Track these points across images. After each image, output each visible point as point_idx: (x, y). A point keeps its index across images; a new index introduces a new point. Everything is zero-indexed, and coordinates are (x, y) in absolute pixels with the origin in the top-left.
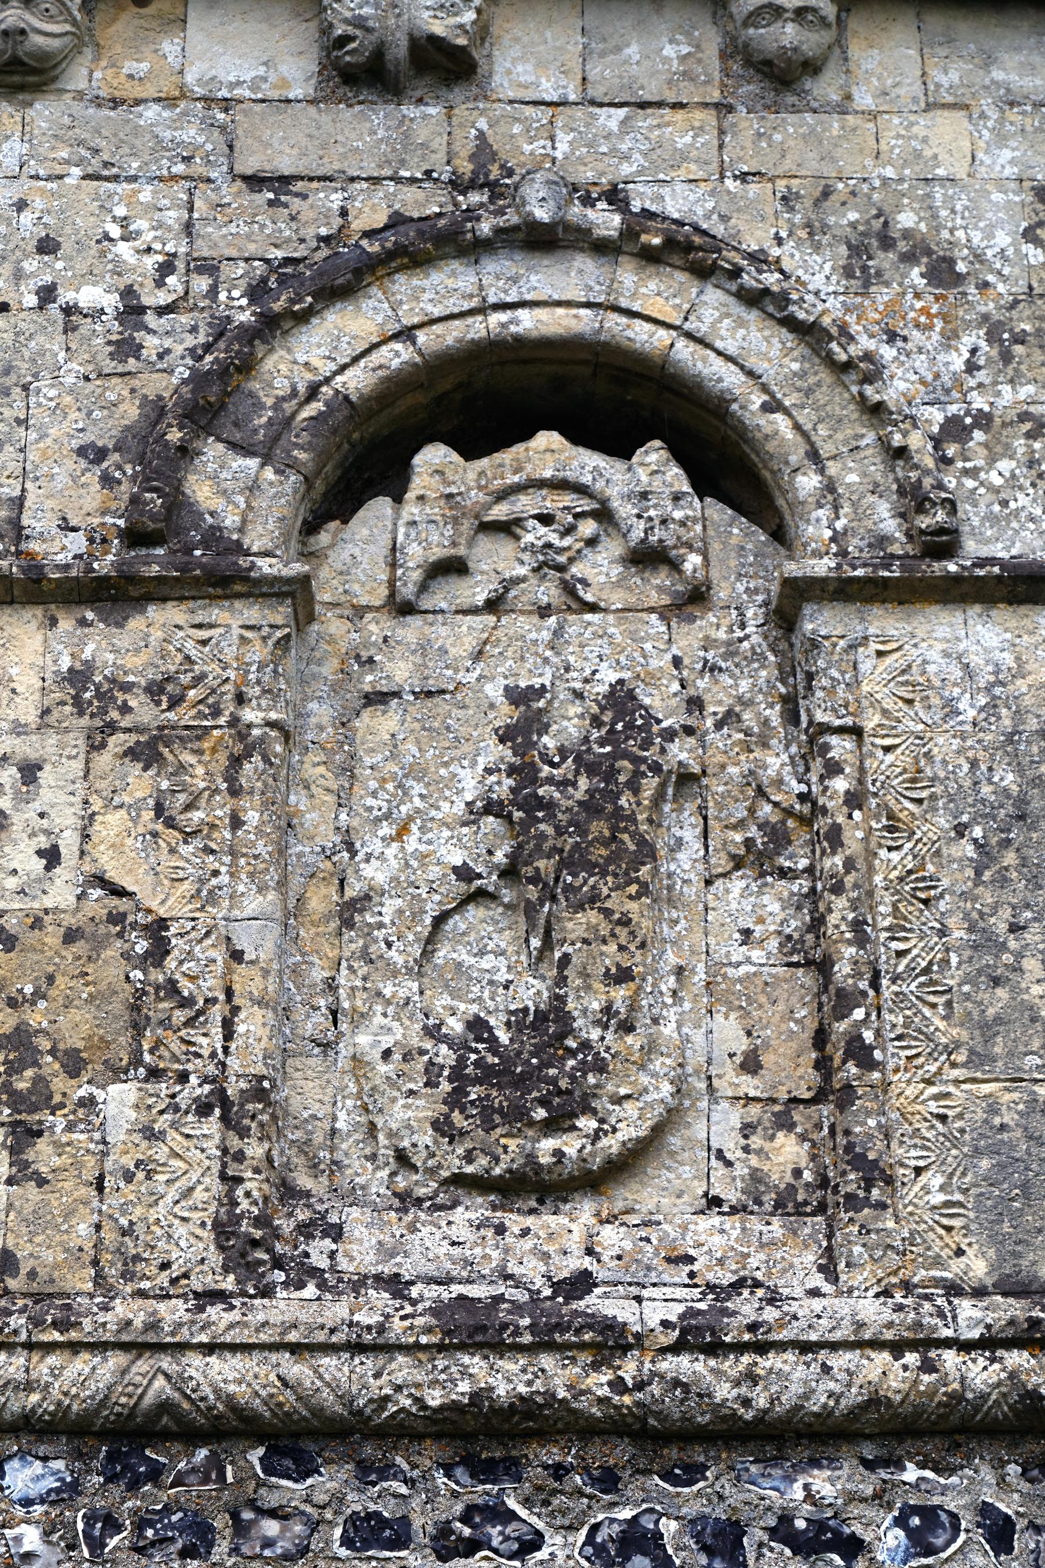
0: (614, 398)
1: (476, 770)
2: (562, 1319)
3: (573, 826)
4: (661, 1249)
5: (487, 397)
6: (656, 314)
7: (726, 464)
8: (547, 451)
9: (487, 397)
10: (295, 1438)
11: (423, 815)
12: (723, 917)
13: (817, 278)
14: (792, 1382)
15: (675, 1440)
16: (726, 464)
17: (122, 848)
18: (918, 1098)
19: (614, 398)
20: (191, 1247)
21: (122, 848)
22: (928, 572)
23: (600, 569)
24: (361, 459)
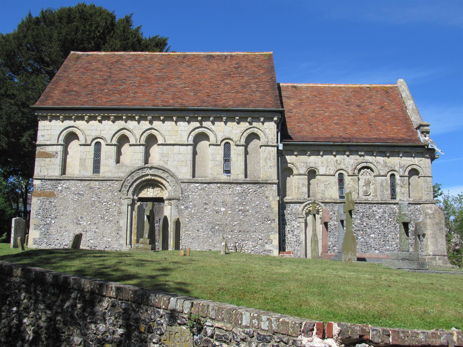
0: (368, 168)
1: (364, 181)
2: (367, 200)
3: (368, 183)
4: (370, 198)
5: (363, 168)
6: (369, 165)
7: (372, 170)
8: (366, 170)
9: (363, 168)
10: (360, 203)
11: (362, 182)
12: (372, 187)
13: (375, 164)
14: (374, 202)
15: (371, 203)
16: (372, 170)
17: (353, 185)
18: (379, 193)
19: (368, 168)
20: (356, 197)
21: (353, 185)
22: (379, 176)
23: (368, 174)
24: (360, 170)
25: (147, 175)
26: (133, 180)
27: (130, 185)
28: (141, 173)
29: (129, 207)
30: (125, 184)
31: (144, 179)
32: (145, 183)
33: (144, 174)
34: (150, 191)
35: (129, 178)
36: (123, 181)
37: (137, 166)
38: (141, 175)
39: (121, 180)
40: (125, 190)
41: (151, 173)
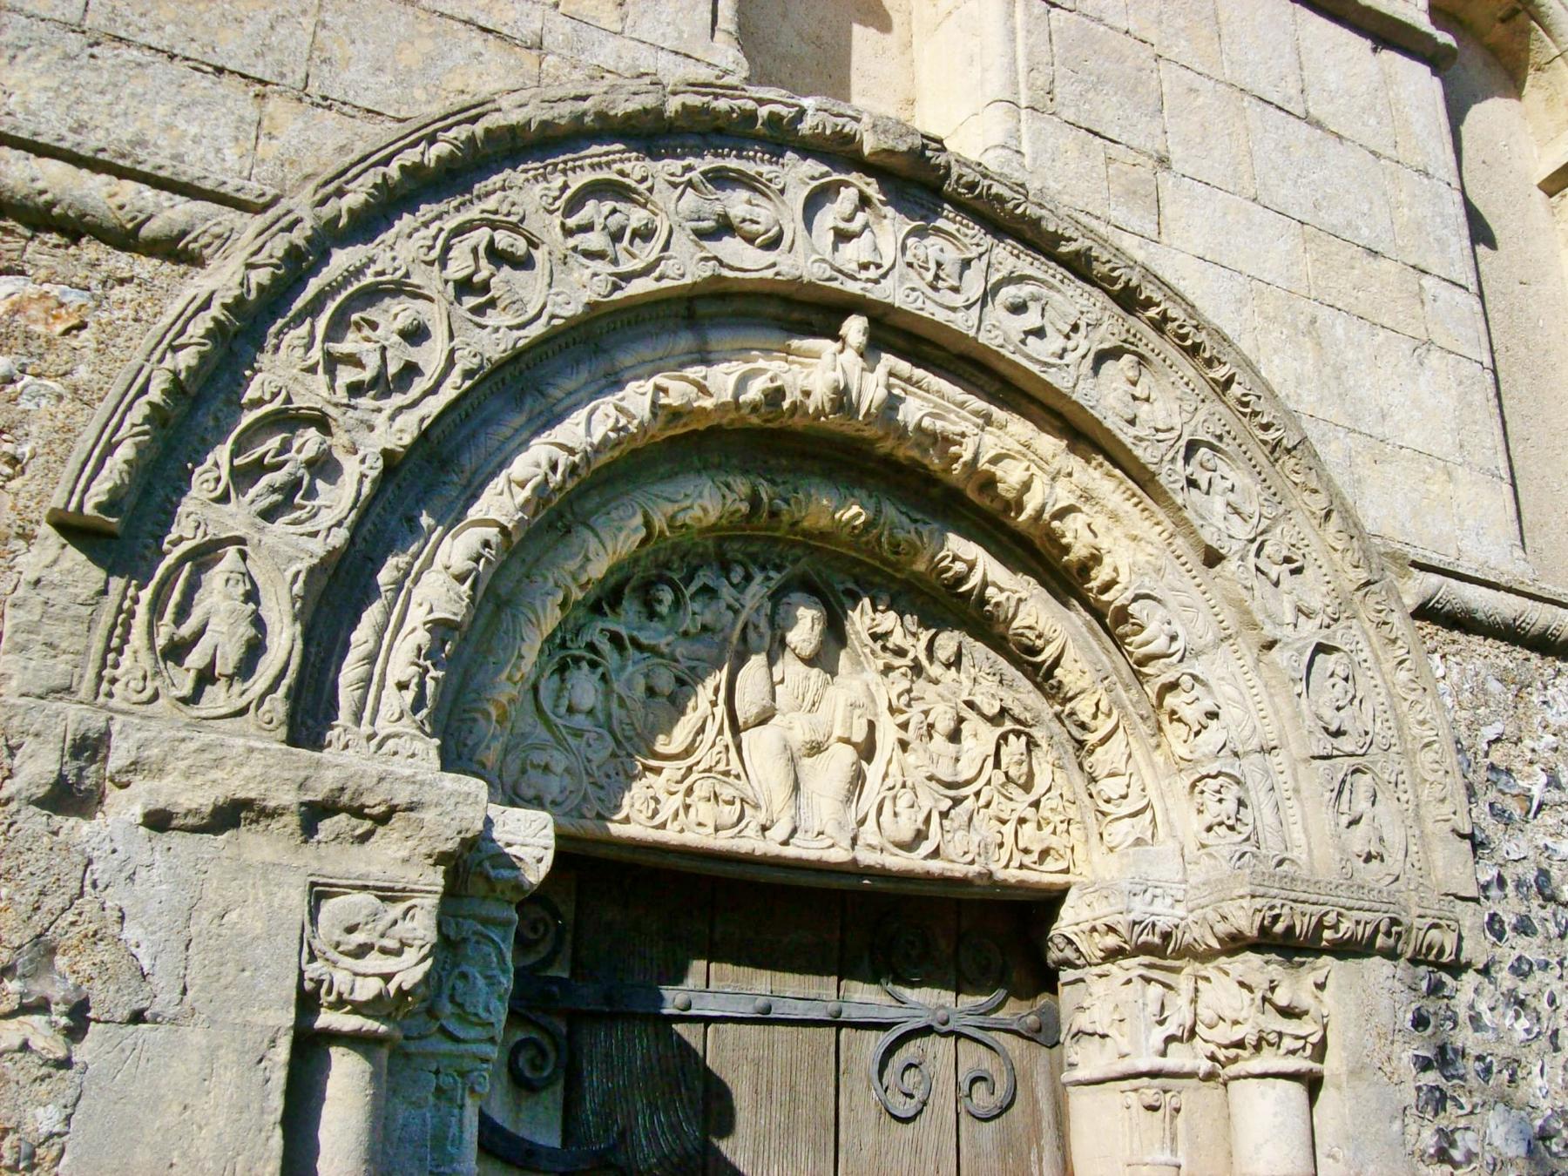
25: (810, 312)
26: (494, 339)
27: (394, 427)
28: (673, 230)
29: (347, 1081)
30: (283, 370)
31: (726, 381)
32: (704, 502)
33: (743, 259)
34: (794, 726)
35: (402, 246)
36: (223, 279)
37: (606, 53)
38: (687, 266)
39: (176, 250)
40: (255, 552)
41: (894, 292)
